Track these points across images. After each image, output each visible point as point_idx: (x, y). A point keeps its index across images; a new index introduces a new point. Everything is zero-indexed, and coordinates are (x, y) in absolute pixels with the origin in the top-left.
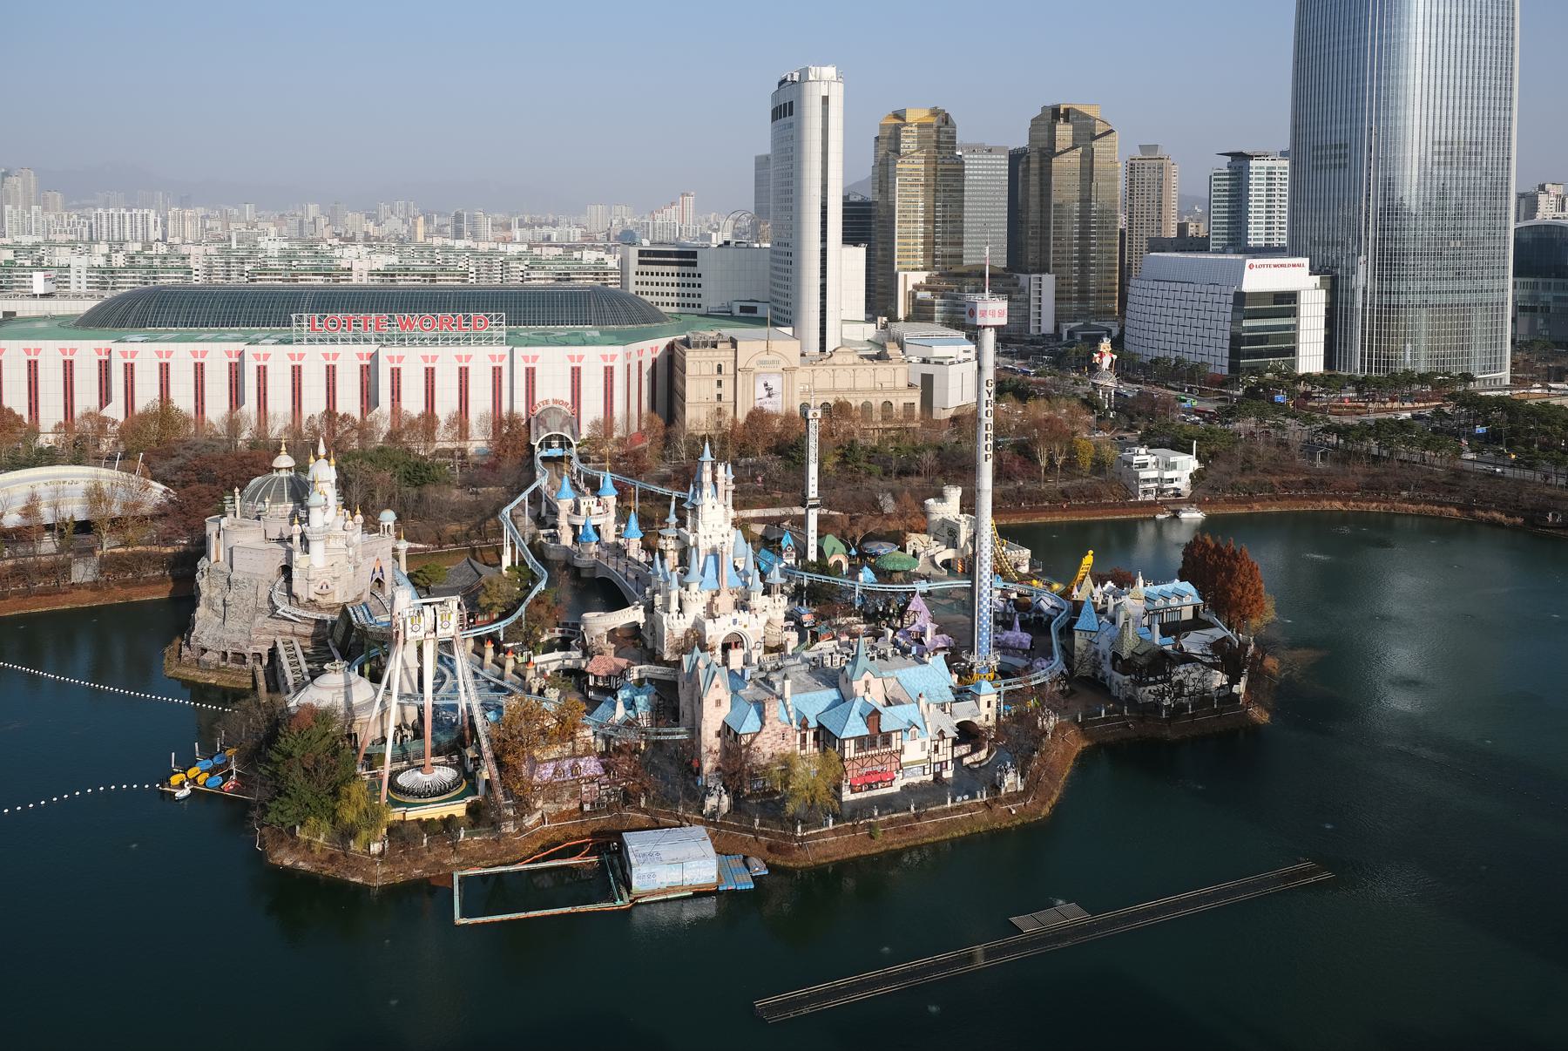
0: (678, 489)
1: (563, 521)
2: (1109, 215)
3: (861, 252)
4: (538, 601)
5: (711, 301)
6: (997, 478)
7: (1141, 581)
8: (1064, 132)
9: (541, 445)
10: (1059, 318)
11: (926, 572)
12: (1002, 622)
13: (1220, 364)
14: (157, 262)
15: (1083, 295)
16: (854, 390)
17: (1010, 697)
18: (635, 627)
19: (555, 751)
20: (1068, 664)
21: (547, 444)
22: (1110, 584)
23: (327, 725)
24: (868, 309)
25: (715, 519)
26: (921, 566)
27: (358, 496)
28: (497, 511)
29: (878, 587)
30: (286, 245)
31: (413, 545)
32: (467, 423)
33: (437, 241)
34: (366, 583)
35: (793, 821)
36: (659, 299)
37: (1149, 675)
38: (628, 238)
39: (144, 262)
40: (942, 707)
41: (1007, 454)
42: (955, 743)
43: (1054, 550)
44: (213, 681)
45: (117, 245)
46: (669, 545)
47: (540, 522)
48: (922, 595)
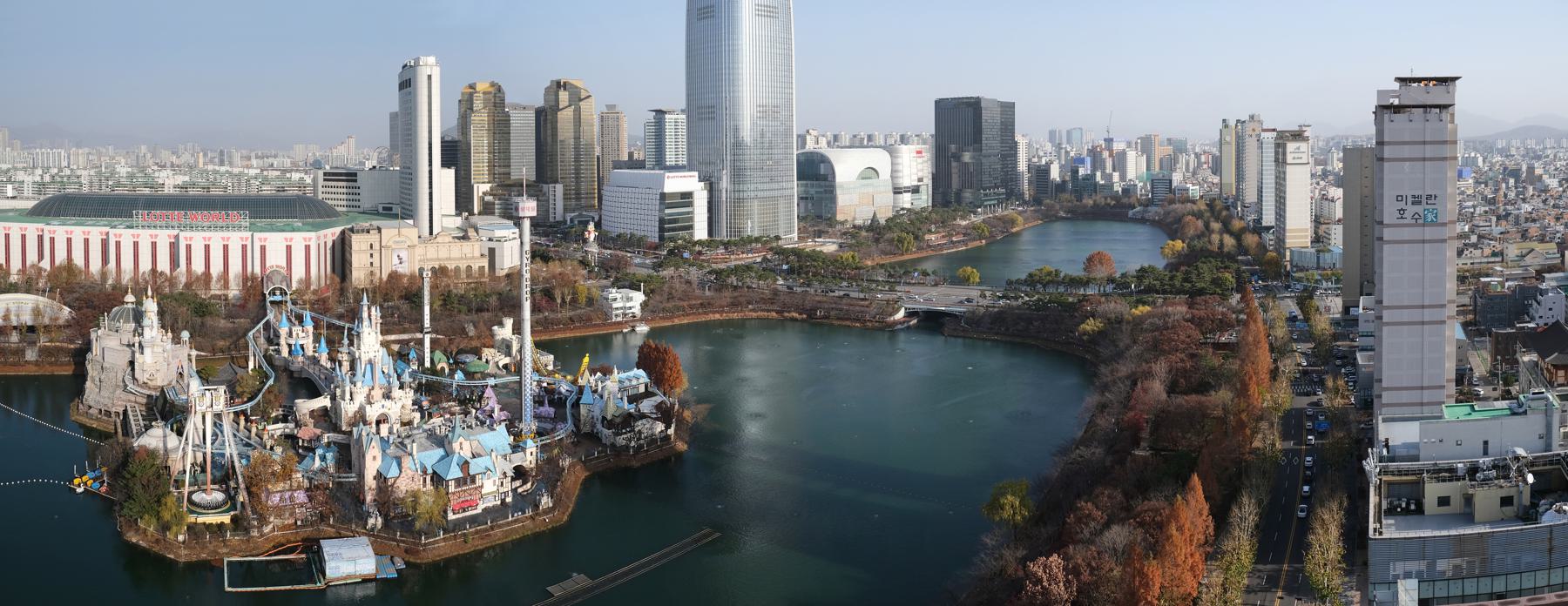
1: (283, 341)
2: (591, 146)
3: (452, 171)
4: (269, 391)
5: (366, 204)
6: (533, 311)
8: (564, 96)
10: (566, 210)
12: (538, 401)
15: (578, 196)
17: (544, 448)
18: (325, 408)
19: (280, 486)
24: (457, 208)
25: (371, 342)
26: (491, 369)
28: (245, 334)
29: (466, 383)
33: (210, 167)
38: (317, 165)
40: (505, 457)
41: (538, 296)
42: (513, 479)
43: (566, 353)
46: (344, 357)
47: (270, 341)
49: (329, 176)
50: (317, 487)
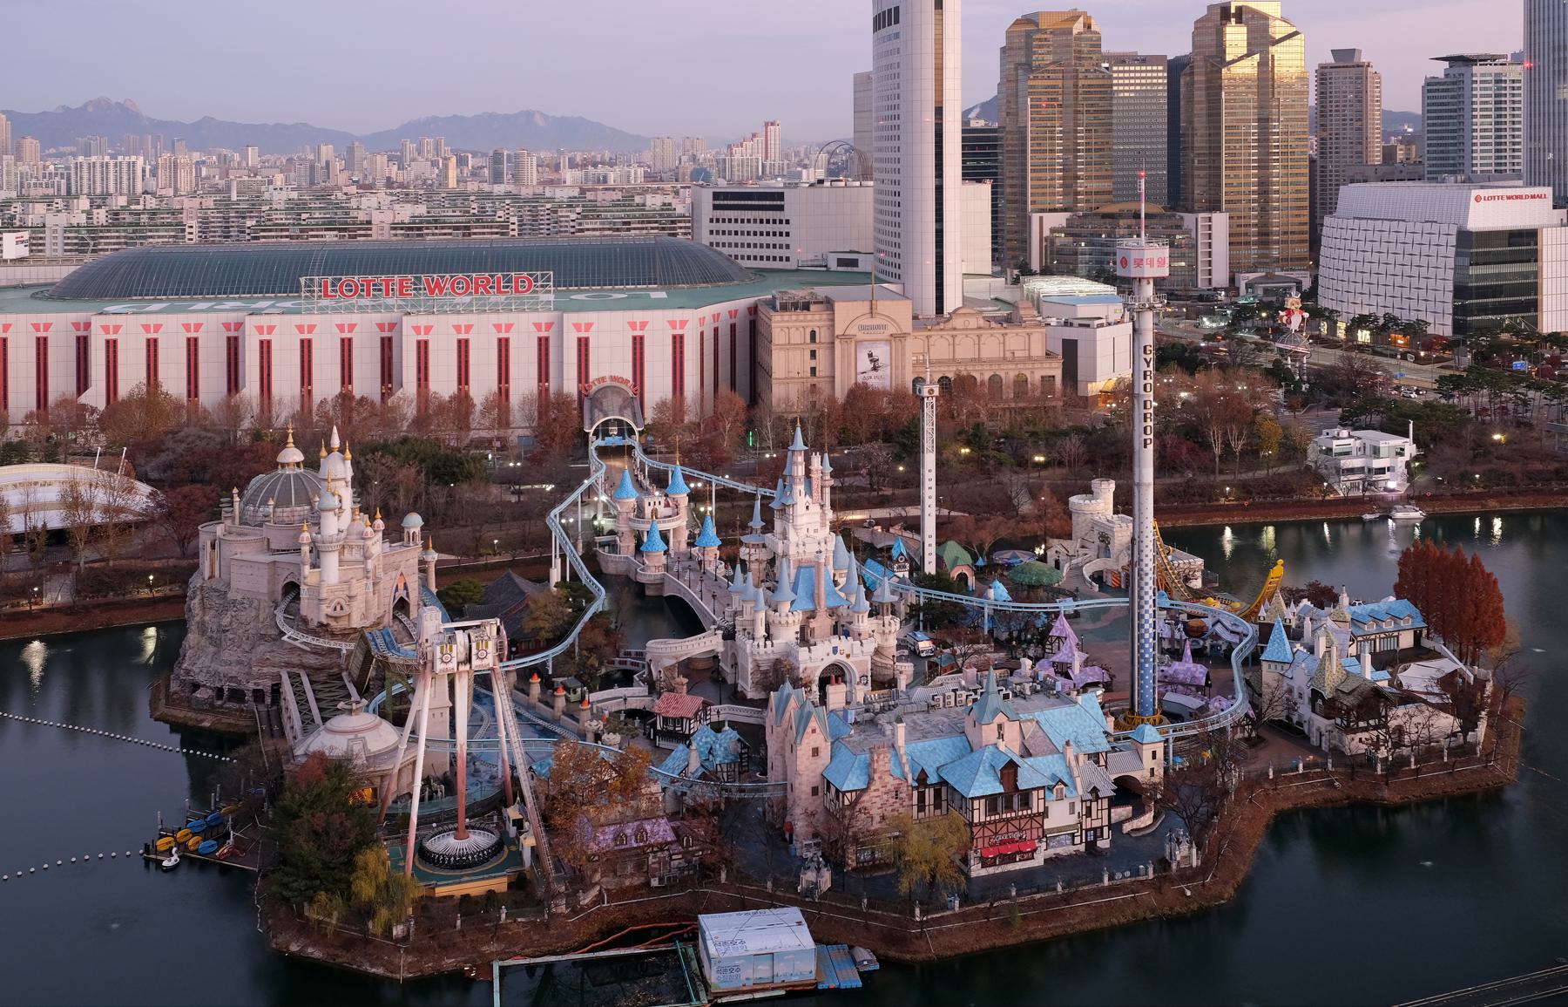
0: (764, 485)
3: (985, 189)
7: (1345, 599)
9: (596, 433)
10: (1235, 268)
11: (1071, 587)
13: (1442, 327)
14: (144, 218)
16: (978, 360)
20: (1254, 706)
21: (603, 431)
22: (1305, 602)
23: (341, 779)
24: (995, 260)
25: (808, 526)
27: (381, 501)
29: (1012, 607)
30: (295, 195)
31: (445, 557)
32: (507, 407)
33: (472, 186)
34: (388, 604)
35: (909, 901)
36: (739, 251)
37: (1358, 719)
39: (129, 219)
40: (1095, 757)
41: (1169, 439)
44: (206, 724)
45: (99, 200)
48: (1067, 617)
49: (723, 200)
50: (694, 812)
